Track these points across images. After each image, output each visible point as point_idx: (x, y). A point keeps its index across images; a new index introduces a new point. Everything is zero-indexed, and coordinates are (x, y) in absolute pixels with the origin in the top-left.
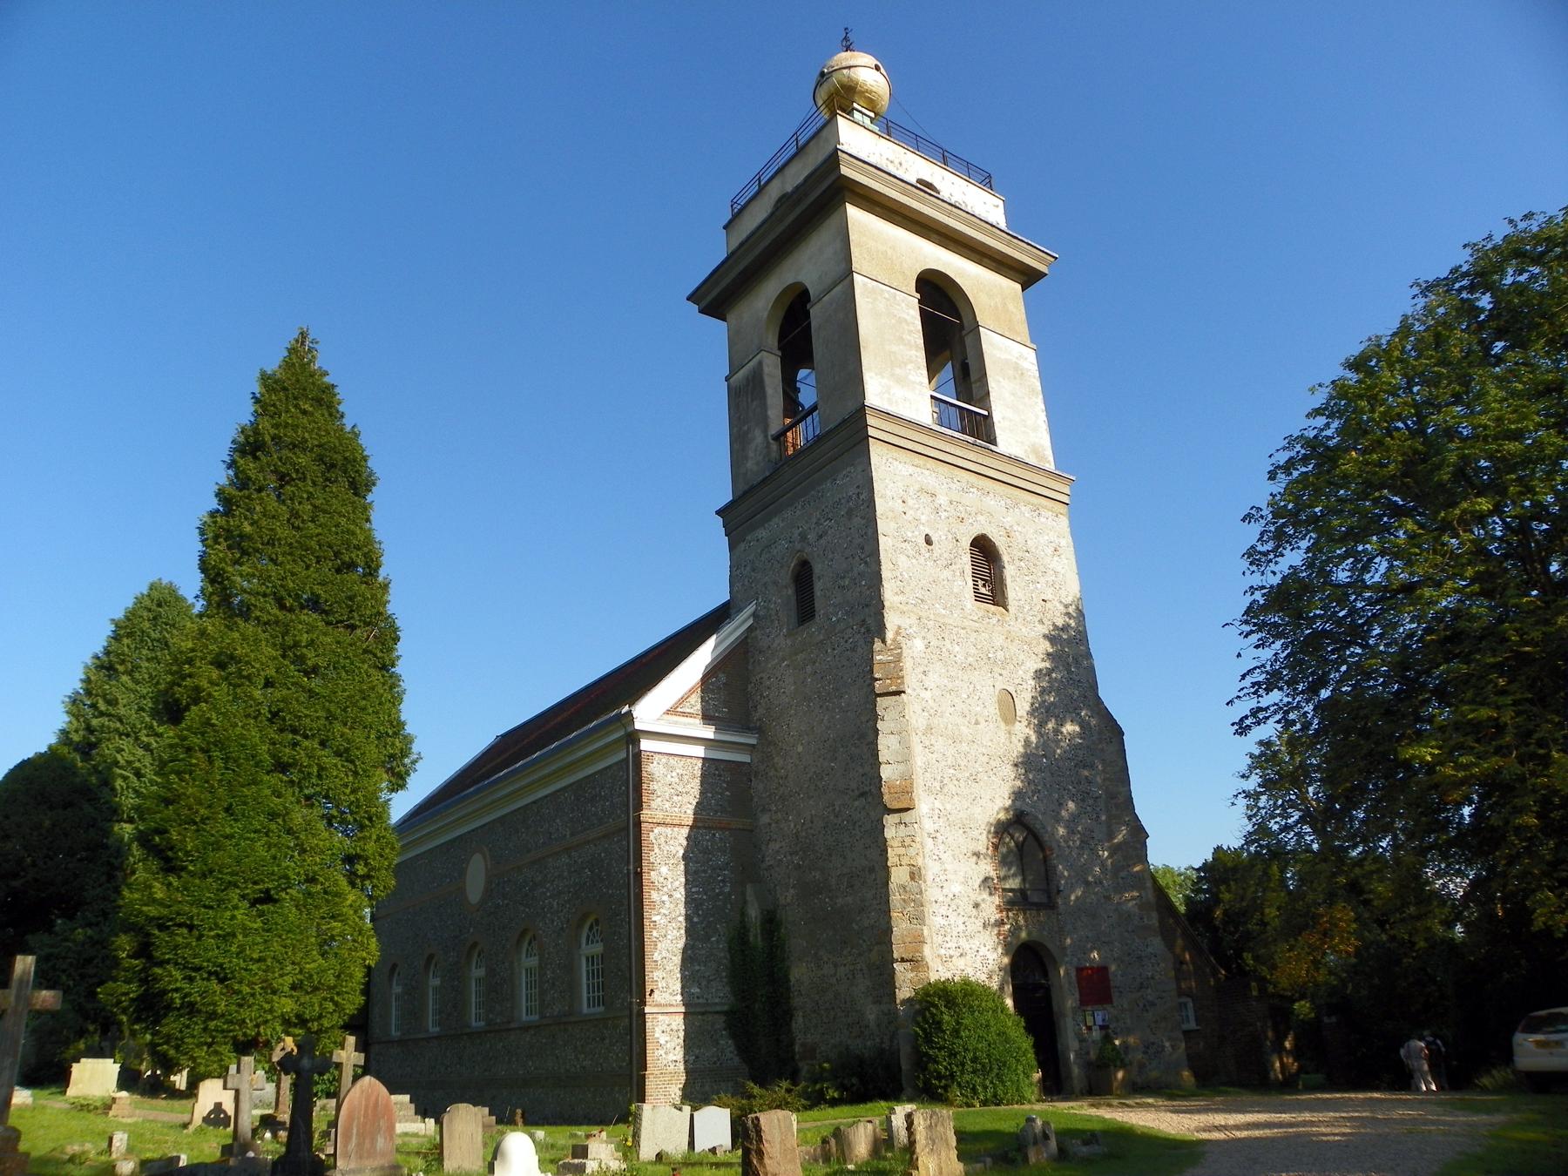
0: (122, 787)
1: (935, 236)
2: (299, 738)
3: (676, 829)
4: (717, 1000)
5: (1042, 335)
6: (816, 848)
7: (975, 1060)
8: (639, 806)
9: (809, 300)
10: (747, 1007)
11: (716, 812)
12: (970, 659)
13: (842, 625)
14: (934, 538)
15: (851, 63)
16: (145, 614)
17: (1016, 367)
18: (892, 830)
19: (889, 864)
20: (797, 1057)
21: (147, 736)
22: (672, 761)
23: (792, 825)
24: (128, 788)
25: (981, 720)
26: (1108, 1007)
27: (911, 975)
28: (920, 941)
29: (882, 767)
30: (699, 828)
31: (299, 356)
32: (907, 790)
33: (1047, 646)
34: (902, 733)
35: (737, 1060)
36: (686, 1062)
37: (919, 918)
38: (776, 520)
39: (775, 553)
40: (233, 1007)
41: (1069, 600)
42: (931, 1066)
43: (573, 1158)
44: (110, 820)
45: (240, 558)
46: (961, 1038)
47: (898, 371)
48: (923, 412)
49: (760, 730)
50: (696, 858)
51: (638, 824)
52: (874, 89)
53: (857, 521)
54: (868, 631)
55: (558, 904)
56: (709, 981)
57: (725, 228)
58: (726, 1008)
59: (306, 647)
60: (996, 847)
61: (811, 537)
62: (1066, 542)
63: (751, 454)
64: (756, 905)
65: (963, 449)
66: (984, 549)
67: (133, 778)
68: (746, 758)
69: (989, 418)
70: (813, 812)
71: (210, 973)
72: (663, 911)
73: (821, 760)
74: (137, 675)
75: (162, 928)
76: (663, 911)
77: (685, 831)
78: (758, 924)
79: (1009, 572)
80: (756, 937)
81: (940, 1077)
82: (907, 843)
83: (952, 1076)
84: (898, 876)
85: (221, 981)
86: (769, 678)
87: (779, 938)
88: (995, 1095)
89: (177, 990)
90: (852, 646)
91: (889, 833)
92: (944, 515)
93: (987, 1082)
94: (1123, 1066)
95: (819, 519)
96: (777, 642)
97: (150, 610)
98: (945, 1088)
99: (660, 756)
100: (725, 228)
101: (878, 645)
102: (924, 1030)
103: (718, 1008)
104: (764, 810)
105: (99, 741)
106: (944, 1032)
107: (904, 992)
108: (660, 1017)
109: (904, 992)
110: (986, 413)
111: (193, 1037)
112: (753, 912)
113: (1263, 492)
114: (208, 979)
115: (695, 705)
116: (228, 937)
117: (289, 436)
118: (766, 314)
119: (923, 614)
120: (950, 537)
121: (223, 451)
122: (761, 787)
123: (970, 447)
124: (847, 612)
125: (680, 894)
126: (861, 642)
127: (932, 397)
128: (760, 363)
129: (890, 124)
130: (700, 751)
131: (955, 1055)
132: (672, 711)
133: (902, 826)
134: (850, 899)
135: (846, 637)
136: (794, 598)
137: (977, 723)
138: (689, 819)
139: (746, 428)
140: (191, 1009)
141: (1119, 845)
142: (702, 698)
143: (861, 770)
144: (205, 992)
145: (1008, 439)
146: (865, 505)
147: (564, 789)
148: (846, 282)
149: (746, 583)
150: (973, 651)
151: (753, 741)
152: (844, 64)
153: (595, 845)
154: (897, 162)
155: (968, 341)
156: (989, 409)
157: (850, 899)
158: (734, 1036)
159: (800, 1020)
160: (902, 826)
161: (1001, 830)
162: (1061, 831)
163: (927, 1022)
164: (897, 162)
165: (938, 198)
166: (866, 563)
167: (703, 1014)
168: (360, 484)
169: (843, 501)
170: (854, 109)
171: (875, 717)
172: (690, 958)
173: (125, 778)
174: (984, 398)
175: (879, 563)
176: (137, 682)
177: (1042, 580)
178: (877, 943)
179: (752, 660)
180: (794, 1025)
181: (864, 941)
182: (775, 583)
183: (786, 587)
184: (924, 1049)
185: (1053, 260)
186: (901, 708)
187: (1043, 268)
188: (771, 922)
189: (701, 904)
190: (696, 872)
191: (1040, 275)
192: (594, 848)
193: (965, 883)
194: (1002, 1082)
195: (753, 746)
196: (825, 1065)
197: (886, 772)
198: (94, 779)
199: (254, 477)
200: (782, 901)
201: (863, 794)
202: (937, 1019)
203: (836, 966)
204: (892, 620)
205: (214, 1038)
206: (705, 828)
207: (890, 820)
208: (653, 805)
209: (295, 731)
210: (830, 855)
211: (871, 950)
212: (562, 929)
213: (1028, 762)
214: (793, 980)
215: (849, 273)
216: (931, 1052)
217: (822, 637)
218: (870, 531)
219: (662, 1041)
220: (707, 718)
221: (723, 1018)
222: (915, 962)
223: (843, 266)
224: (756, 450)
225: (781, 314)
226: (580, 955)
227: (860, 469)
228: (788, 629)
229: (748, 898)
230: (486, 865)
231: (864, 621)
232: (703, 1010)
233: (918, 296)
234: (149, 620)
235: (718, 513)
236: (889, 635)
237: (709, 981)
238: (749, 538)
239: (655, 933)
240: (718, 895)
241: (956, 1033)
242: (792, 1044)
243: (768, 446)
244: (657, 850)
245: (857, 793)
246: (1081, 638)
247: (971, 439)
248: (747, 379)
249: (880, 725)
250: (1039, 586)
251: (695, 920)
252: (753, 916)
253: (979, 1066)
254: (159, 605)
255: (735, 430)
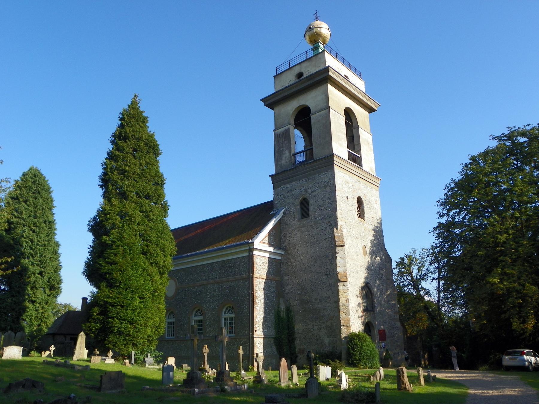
0: (25, 246)
1: (349, 96)
2: (148, 243)
3: (262, 280)
4: (272, 334)
5: (374, 131)
6: (307, 289)
7: (367, 356)
8: (253, 272)
9: (311, 113)
10: (280, 336)
11: (272, 275)
12: (357, 236)
13: (321, 222)
14: (349, 197)
15: (321, 26)
16: (30, 180)
17: (367, 141)
18: (341, 286)
19: (340, 297)
20: (297, 352)
21: (34, 226)
22: (261, 258)
23: (297, 281)
24: (28, 246)
25: (359, 254)
26: (385, 341)
27: (346, 330)
28: (349, 320)
29: (338, 268)
30: (267, 279)
31: (134, 105)
32: (345, 276)
33: (373, 233)
34: (343, 258)
35: (276, 352)
36: (264, 353)
37: (348, 314)
38: (294, 183)
39: (294, 193)
40: (135, 333)
41: (378, 218)
42: (354, 357)
43: (408, 377)
44: (20, 258)
45: (124, 178)
46: (363, 349)
47: (340, 142)
48: (346, 157)
49: (285, 249)
50: (266, 290)
51: (252, 277)
52: (327, 36)
53: (328, 189)
54: (331, 225)
55: (213, 300)
56: (270, 328)
57: (274, 77)
58: (274, 336)
59: (149, 212)
60: (361, 294)
61: (309, 191)
62: (378, 199)
63: (284, 158)
64: (284, 305)
65: (353, 166)
66: (360, 201)
67: (30, 242)
68: (279, 258)
69: (360, 158)
70: (306, 278)
71: (128, 321)
72: (259, 305)
73: (310, 262)
74: (28, 203)
75: (113, 306)
76: (259, 305)
77: (264, 281)
78: (284, 310)
79: (365, 208)
80: (283, 314)
81: (356, 360)
82: (345, 291)
83: (360, 360)
84: (342, 301)
85: (131, 324)
86: (290, 234)
87: (291, 316)
88: (371, 366)
89: (116, 327)
90: (325, 228)
91: (340, 288)
92: (351, 190)
93: (369, 362)
94: (391, 359)
95: (313, 186)
96: (293, 222)
97: (32, 178)
98: (358, 363)
99: (258, 256)
100: (274, 77)
101: (335, 230)
102: (351, 346)
103: (272, 336)
104: (286, 275)
105: (16, 227)
106: (358, 347)
107: (344, 335)
108: (258, 339)
109: (344, 335)
110: (359, 156)
111: (120, 342)
112: (283, 307)
113: (441, 195)
114: (127, 324)
115: (267, 240)
116: (134, 310)
117: (138, 135)
118: (291, 112)
119: (346, 221)
120: (352, 197)
121: (109, 137)
122: (285, 267)
123: (358, 168)
124: (323, 218)
125: (263, 301)
126: (328, 228)
127: (348, 151)
128: (289, 129)
129: (331, 49)
130: (268, 255)
131: (361, 354)
132: (261, 242)
133: (344, 286)
134: (320, 306)
135: (322, 226)
136: (300, 209)
137: (358, 255)
138: (265, 277)
139: (282, 149)
140: (120, 333)
141: (389, 295)
142: (269, 238)
143: (326, 267)
144: (126, 327)
145: (365, 166)
146: (331, 185)
147: (216, 262)
148: (327, 110)
149: (281, 201)
150: (357, 233)
151: (283, 253)
152: (319, 26)
153: (232, 283)
154: (339, 69)
155: (354, 131)
156: (360, 155)
157: (320, 306)
158: (276, 345)
159: (298, 341)
160: (344, 286)
161: (363, 288)
162: (375, 290)
163: (352, 344)
164: (339, 69)
165: (348, 80)
166: (331, 203)
167: (268, 338)
168: (157, 153)
169: (322, 182)
170: (319, 42)
171: (336, 253)
172: (265, 320)
173: (27, 242)
174: (359, 151)
175: (336, 205)
176: (28, 206)
177: (373, 211)
178: (330, 320)
179: (282, 227)
180: (296, 343)
181: (325, 319)
182: (293, 203)
183: (297, 205)
184: (352, 352)
185: (379, 106)
186: (343, 251)
187: (376, 108)
188: (288, 310)
189: (268, 304)
190: (267, 294)
191: (375, 110)
192: (231, 283)
193: (355, 303)
194: (373, 362)
195: (282, 254)
196: (317, 355)
197: (339, 270)
198: (12, 242)
199: (125, 149)
200: (292, 304)
201: (327, 275)
202: (356, 343)
203: (313, 326)
204: (340, 223)
205: (127, 342)
206: (269, 280)
207: (340, 284)
208: (256, 272)
209: (147, 241)
210: (313, 292)
211: (327, 322)
212: (215, 308)
213: (369, 268)
214: (296, 329)
215: (328, 107)
216: (354, 353)
217: (312, 224)
218: (333, 194)
219: (258, 346)
220: (270, 245)
221: (273, 340)
222: (347, 326)
223: (325, 104)
224: (286, 158)
225: (296, 113)
226: (222, 318)
227: (330, 173)
228: (298, 219)
229: (281, 302)
230: (176, 284)
231: (330, 221)
232: (268, 337)
233: (345, 116)
234: (32, 182)
235: (270, 176)
236: (339, 227)
237: (270, 328)
238: (282, 186)
239: (257, 313)
240: (272, 301)
241: (361, 348)
242: (295, 348)
243: (291, 157)
244: (257, 286)
245: (324, 274)
246: (381, 230)
247: (358, 166)
248: (283, 133)
249: (337, 255)
250: (372, 213)
251: (267, 309)
252: (283, 308)
253: (368, 358)
254: (35, 176)
255: (277, 149)
